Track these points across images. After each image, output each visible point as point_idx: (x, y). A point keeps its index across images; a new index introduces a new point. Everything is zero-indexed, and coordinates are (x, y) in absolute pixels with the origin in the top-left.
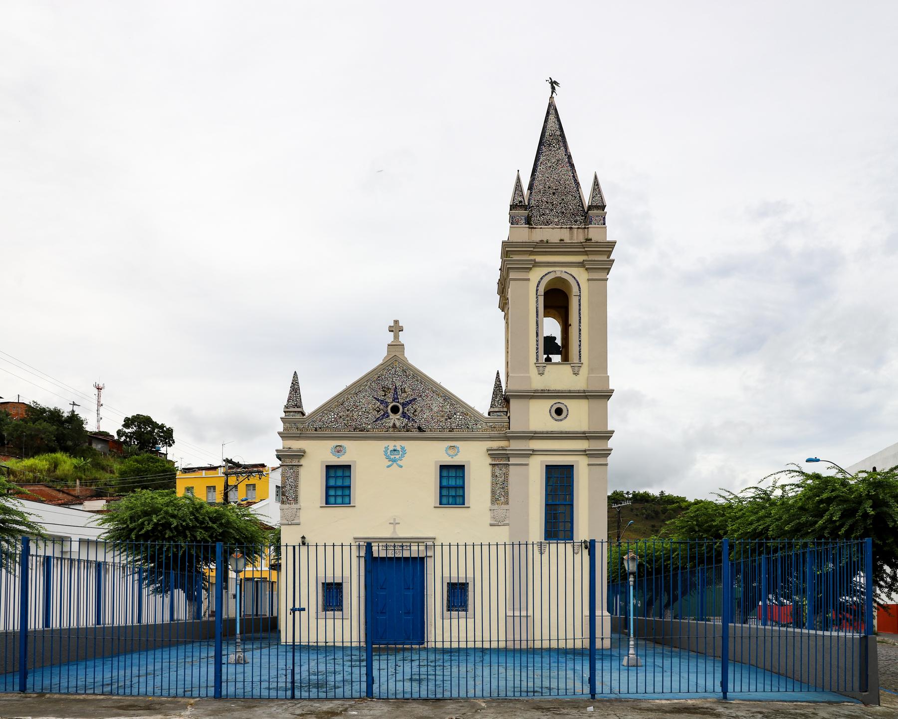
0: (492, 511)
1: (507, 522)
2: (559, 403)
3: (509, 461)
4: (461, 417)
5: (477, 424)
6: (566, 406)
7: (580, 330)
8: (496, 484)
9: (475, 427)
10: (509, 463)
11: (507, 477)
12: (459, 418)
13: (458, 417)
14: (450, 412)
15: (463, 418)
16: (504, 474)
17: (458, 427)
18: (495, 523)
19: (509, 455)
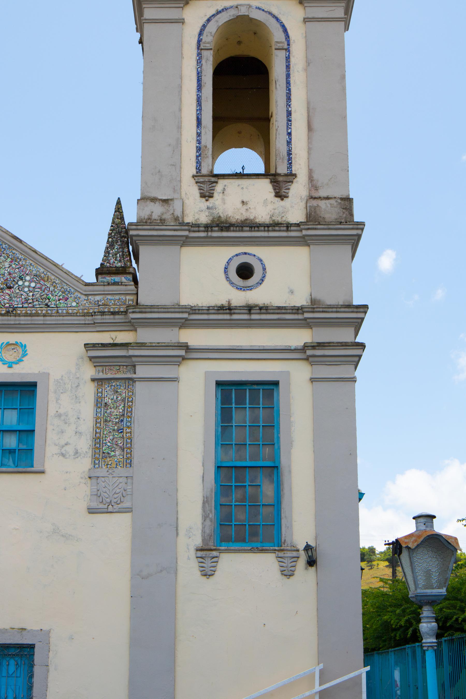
0: (94, 481)
1: (127, 504)
2: (245, 253)
3: (135, 373)
4: (33, 285)
5: (67, 299)
6: (261, 260)
7: (289, 114)
8: (106, 421)
9: (62, 304)
10: (134, 376)
11: (130, 407)
12: (29, 286)
13: (27, 284)
14: (10, 274)
15: (38, 285)
16: (123, 400)
17: (26, 305)
18: (101, 506)
19: (134, 359)
